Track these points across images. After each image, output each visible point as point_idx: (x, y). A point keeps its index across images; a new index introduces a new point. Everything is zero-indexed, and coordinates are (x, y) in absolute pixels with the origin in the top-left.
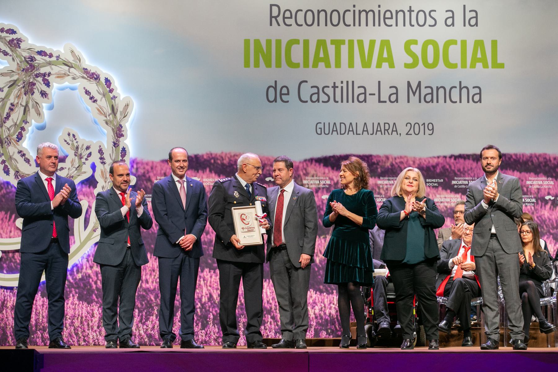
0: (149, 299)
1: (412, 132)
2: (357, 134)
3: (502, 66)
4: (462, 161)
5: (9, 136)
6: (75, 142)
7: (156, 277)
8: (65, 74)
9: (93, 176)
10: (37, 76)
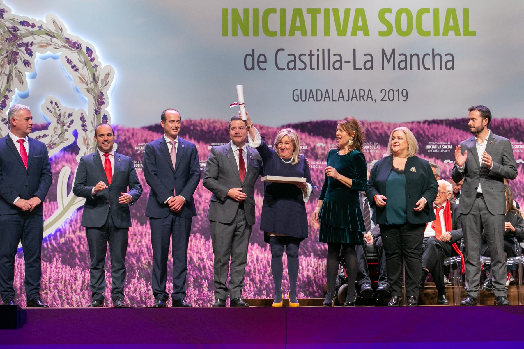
0: (130, 263)
1: (386, 98)
2: (333, 100)
3: (473, 33)
4: (435, 126)
6: (57, 109)
7: (137, 241)
8: (47, 44)
9: (75, 143)
10: (20, 45)
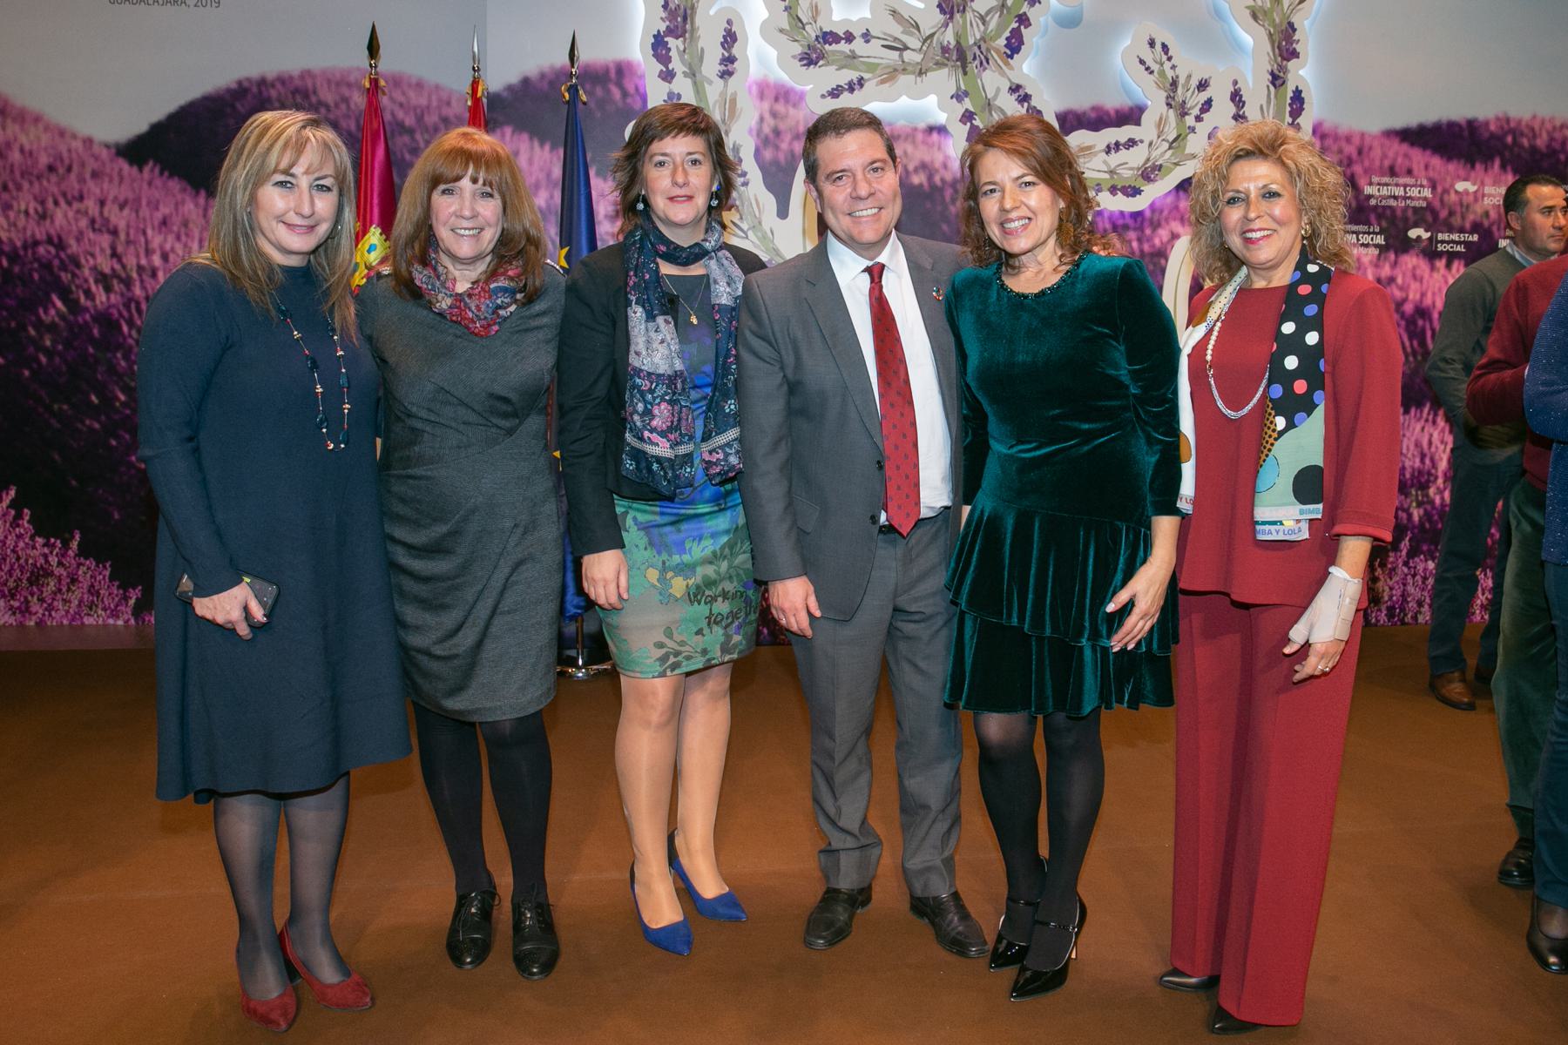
5: (983, 39)
6: (1167, 65)
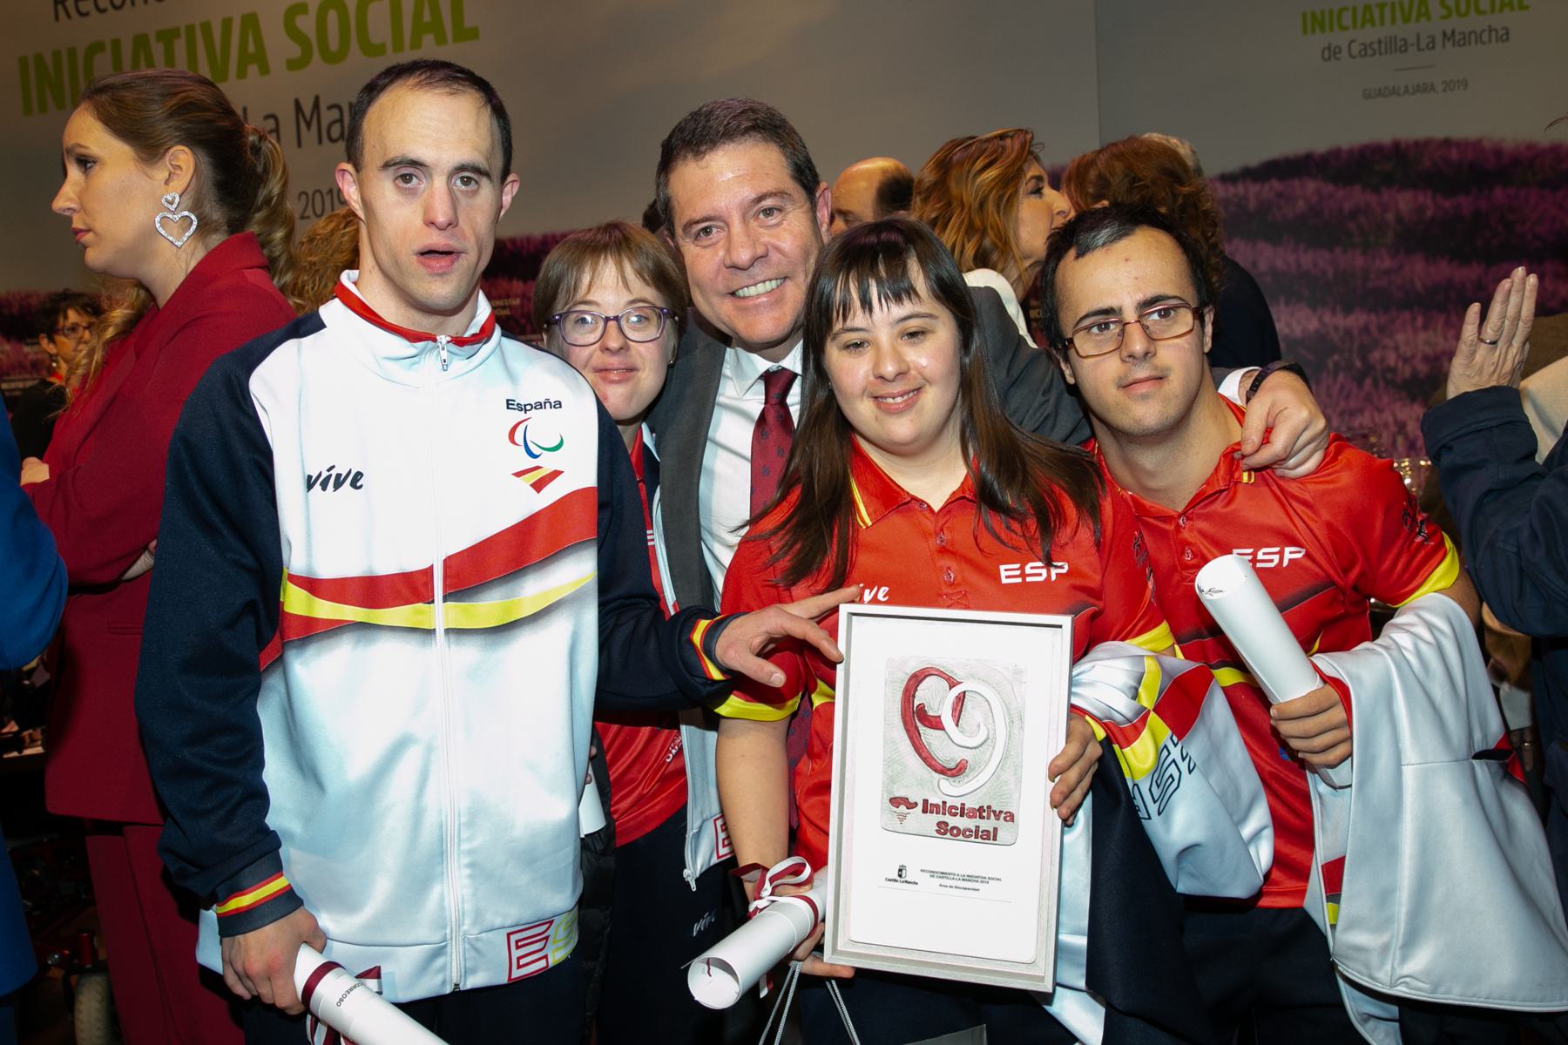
1: (309, 212)
3: (473, 34)
